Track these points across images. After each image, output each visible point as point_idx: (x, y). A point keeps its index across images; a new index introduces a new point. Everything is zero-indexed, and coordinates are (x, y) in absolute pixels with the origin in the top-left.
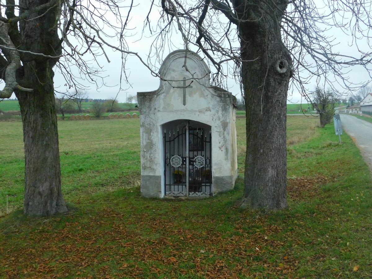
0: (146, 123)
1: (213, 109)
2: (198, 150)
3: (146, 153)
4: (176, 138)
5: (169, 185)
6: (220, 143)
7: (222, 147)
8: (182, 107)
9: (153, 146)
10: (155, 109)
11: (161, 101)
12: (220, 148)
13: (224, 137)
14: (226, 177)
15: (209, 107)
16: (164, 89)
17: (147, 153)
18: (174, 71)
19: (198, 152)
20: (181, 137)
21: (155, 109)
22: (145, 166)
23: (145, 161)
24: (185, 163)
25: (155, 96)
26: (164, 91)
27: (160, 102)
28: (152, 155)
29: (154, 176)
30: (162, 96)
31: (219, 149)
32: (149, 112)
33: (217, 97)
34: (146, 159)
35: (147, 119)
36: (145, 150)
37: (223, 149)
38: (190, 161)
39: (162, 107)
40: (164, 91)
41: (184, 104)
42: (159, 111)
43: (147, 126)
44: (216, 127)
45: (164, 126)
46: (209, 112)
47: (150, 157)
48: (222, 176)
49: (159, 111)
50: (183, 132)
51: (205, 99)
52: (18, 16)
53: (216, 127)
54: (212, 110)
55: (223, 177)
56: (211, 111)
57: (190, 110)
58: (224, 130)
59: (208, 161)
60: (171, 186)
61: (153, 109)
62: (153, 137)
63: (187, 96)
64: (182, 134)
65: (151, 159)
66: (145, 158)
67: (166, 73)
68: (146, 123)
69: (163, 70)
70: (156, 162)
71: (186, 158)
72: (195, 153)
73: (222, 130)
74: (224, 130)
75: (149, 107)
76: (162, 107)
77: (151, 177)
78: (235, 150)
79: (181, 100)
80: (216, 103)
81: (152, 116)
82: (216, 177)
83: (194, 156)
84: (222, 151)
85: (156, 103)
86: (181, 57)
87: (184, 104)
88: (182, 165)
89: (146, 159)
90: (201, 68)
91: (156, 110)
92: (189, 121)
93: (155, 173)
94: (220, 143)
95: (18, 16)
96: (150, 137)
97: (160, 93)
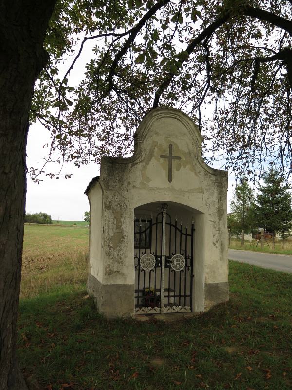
0: (115, 204)
1: (207, 190)
2: (145, 248)
3: (112, 249)
4: (148, 228)
5: (187, 296)
6: (214, 236)
7: (217, 242)
8: (167, 185)
9: (124, 239)
10: (129, 183)
11: (138, 173)
12: (214, 244)
13: (219, 229)
14: (221, 284)
15: (202, 188)
16: (144, 156)
17: (114, 249)
18: (157, 133)
19: (147, 250)
20: (154, 227)
21: (129, 183)
22: (110, 270)
23: (111, 261)
24: (159, 265)
25: (130, 165)
26: (142, 159)
27: (136, 175)
28: (121, 253)
29: (124, 285)
30: (139, 166)
31: (213, 245)
32: (120, 188)
33: (212, 176)
34: (113, 258)
35: (116, 197)
36: (111, 245)
37: (218, 244)
38: (166, 261)
39: (138, 182)
40: (142, 159)
41: (170, 181)
42: (134, 187)
43: (115, 207)
44: (210, 214)
45: (136, 209)
46: (202, 194)
47: (118, 255)
48: (216, 282)
49: (134, 187)
50: (158, 221)
51: (197, 176)
52: (287, 72)
53: (210, 214)
54: (205, 191)
55: (218, 284)
56: (203, 193)
57: (177, 189)
58: (220, 220)
59: (189, 261)
60: (181, 298)
61: (126, 184)
62: (124, 226)
63: (174, 170)
64: (157, 223)
65: (121, 258)
66: (111, 257)
67: (146, 135)
68: (115, 204)
69: (142, 130)
70: (127, 264)
71: (161, 257)
72: (142, 250)
73: (217, 219)
74: (220, 220)
75: (121, 181)
76: (138, 182)
77: (118, 287)
78: (166, 245)
79: (164, 174)
80: (210, 182)
81: (124, 192)
82: (209, 284)
83: (171, 255)
84: (217, 247)
85: (131, 175)
86: (167, 117)
87: (170, 181)
88: (155, 267)
89: (113, 258)
90: (192, 135)
91: (131, 186)
92: (164, 205)
93: (125, 278)
94: (214, 236)
95: (287, 72)
96: (120, 224)
97: (137, 162)
